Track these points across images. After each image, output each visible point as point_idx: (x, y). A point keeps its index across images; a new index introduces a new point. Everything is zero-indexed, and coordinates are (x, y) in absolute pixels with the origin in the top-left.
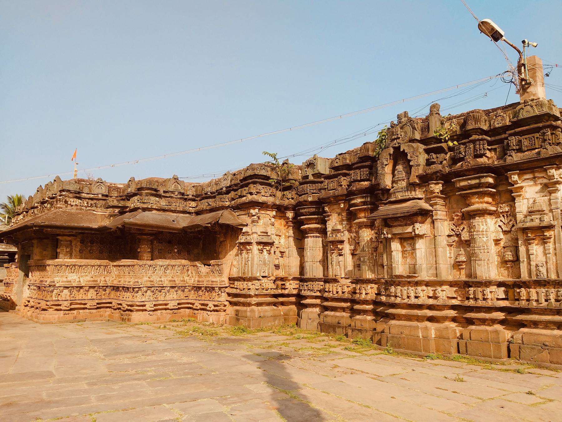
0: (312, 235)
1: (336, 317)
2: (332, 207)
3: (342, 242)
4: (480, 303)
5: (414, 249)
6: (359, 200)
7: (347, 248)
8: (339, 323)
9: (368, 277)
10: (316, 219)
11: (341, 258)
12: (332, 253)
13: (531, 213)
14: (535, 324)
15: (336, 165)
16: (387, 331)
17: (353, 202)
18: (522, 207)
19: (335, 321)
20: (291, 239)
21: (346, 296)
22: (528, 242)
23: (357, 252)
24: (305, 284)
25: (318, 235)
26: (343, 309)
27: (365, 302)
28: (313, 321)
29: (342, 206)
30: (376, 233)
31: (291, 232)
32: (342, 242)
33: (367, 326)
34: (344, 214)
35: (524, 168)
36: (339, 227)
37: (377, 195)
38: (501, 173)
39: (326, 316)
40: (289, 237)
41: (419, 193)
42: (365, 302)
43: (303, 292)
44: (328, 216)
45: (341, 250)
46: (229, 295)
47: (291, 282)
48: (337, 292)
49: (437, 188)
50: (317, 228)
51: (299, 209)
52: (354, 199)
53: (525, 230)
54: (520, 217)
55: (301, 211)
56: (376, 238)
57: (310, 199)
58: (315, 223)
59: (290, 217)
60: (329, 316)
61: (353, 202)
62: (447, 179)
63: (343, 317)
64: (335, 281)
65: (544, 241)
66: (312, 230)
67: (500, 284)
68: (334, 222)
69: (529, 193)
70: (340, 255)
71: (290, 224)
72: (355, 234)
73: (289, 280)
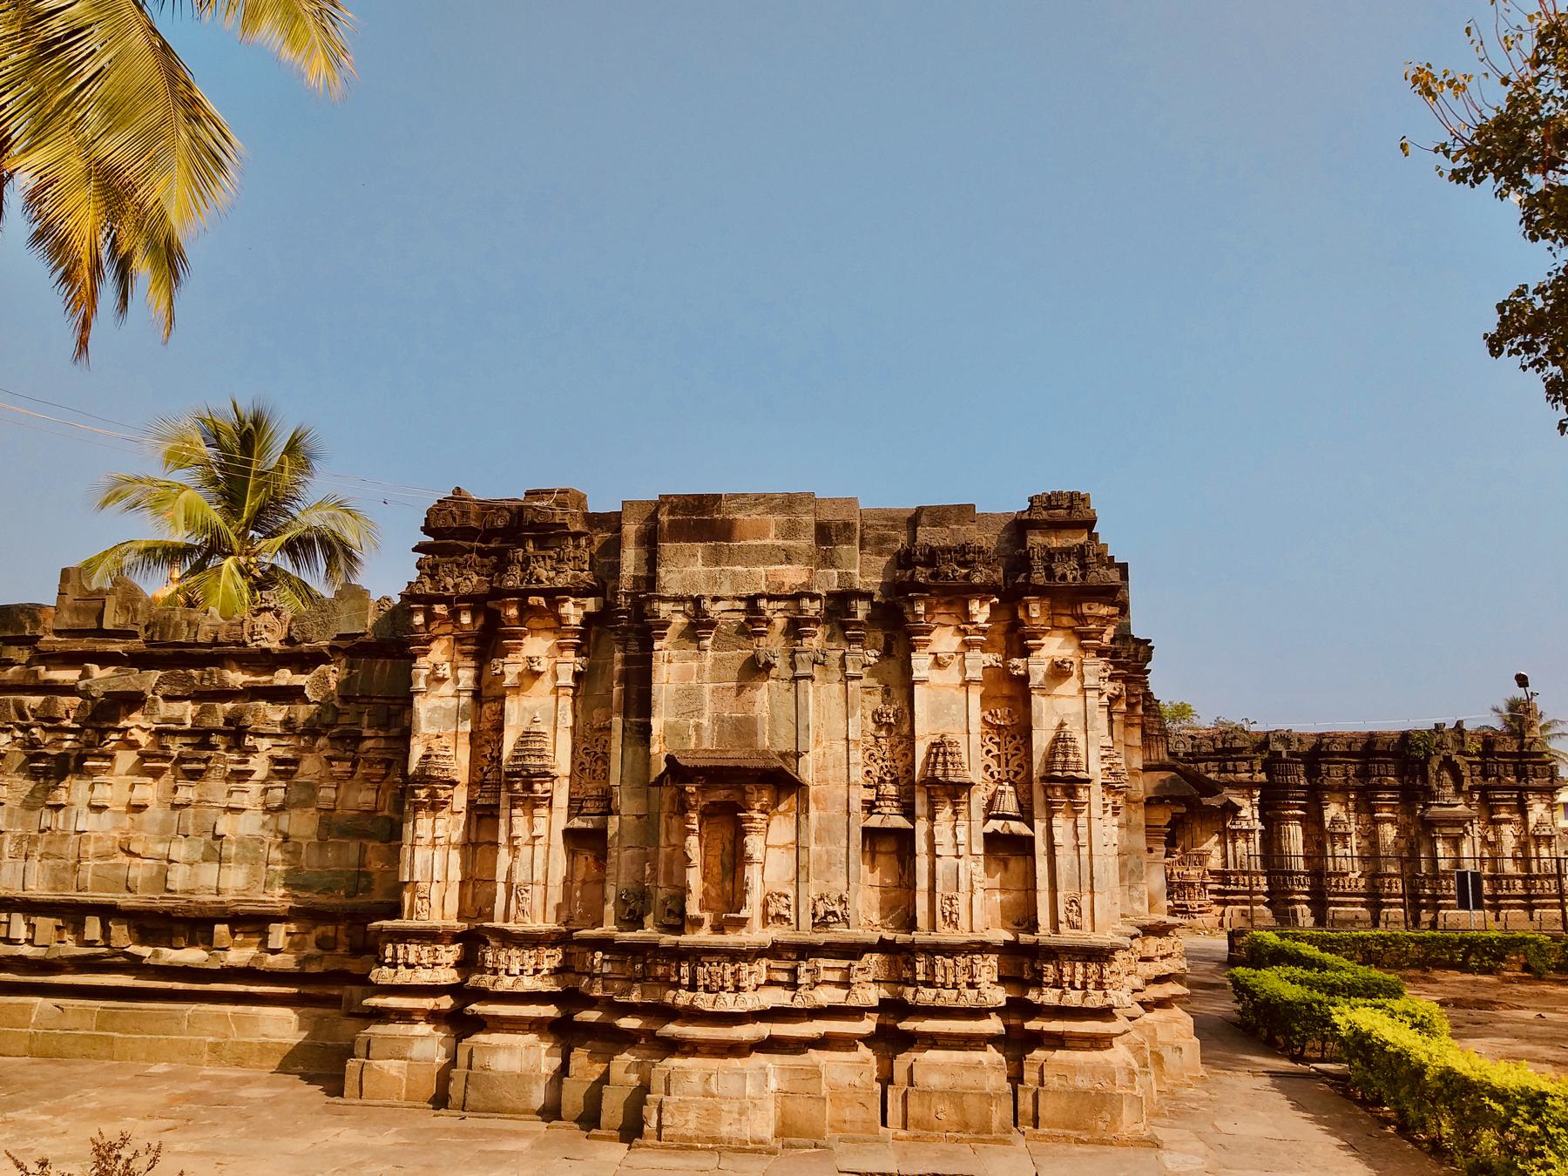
4: (1513, 892)
5: (1457, 848)
7: (1353, 841)
13: (1539, 824)
14: (1544, 906)
16: (1441, 919)
18: (1533, 818)
22: (1538, 846)
26: (1354, 904)
27: (1396, 896)
35: (1538, 790)
37: (1414, 794)
38: (1522, 791)
41: (1461, 800)
42: (1396, 896)
46: (1212, 892)
49: (1477, 797)
53: (1537, 838)
54: (1531, 826)
62: (1485, 790)
65: (1549, 846)
66: (1295, 817)
67: (1518, 877)
68: (1332, 811)
69: (1537, 810)
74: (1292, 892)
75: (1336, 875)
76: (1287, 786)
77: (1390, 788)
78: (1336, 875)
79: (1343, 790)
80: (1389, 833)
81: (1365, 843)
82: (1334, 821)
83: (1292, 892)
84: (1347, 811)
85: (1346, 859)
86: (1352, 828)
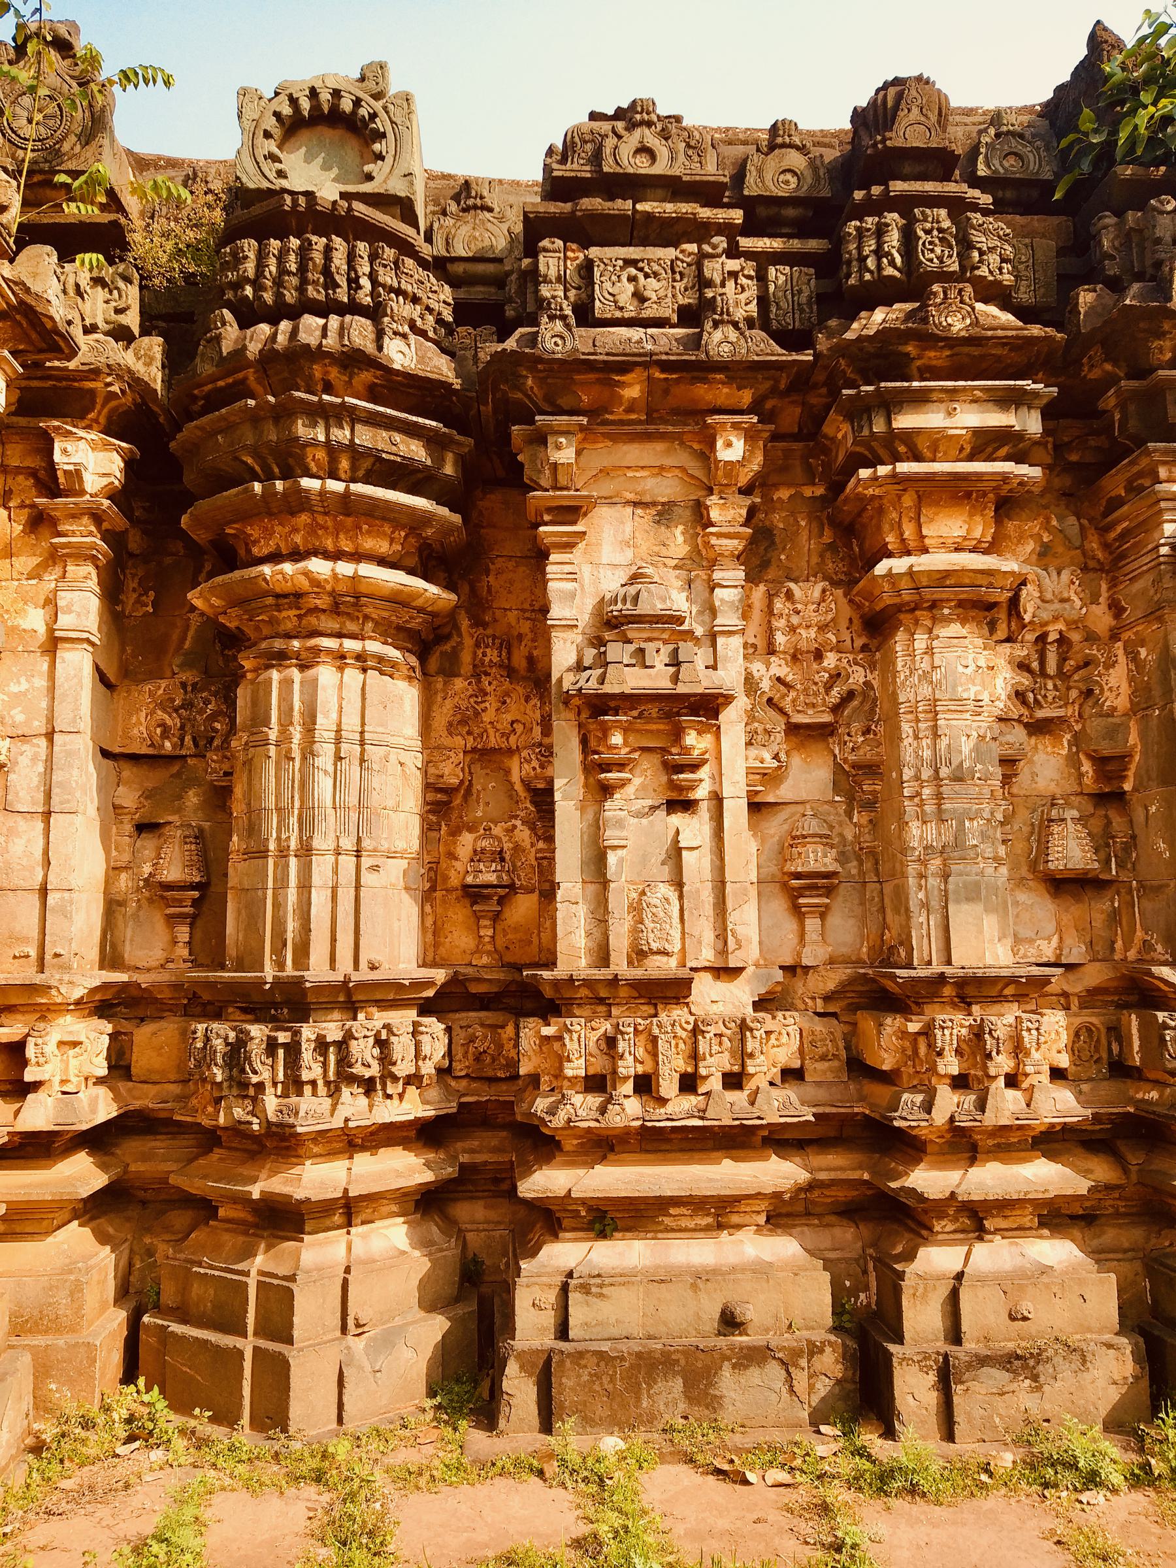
0: (350, 645)
1: (700, 1278)
2: (604, 455)
3: (708, 707)
6: (971, 418)
7: (731, 755)
8: (730, 1322)
9: (989, 961)
10: (414, 522)
11: (694, 829)
12: (606, 790)
15: (642, 166)
17: (905, 421)
19: (688, 1319)
20: (77, 666)
21: (780, 1106)
23: (784, 792)
24: (308, 1032)
25: (394, 653)
28: (387, 1341)
29: (732, 449)
30: (1023, 666)
31: (83, 607)
32: (708, 707)
33: (1049, 1316)
34: (726, 513)
36: (679, 602)
39: (594, 1284)
40: (53, 644)
43: (271, 1102)
44: (571, 513)
45: (694, 767)
47: (70, 1025)
48: (689, 1083)
50: (399, 600)
51: (284, 414)
52: (921, 399)
55: (301, 429)
56: (1019, 695)
57: (401, 354)
58: (382, 562)
59: (92, 483)
60: (625, 1278)
61: (905, 421)
63: (761, 1271)
64: (673, 991)
66: (348, 604)
68: (611, 556)
70: (681, 804)
71: (82, 534)
72: (779, 667)
73: (45, 1013)
74: (281, 1143)
75: (602, 995)
76: (292, 363)
77: (973, 359)
78: (602, 995)
79: (676, 402)
80: (963, 679)
81: (809, 778)
82: (612, 623)
83: (281, 1143)
84: (701, 561)
85: (681, 883)
86: (728, 668)
